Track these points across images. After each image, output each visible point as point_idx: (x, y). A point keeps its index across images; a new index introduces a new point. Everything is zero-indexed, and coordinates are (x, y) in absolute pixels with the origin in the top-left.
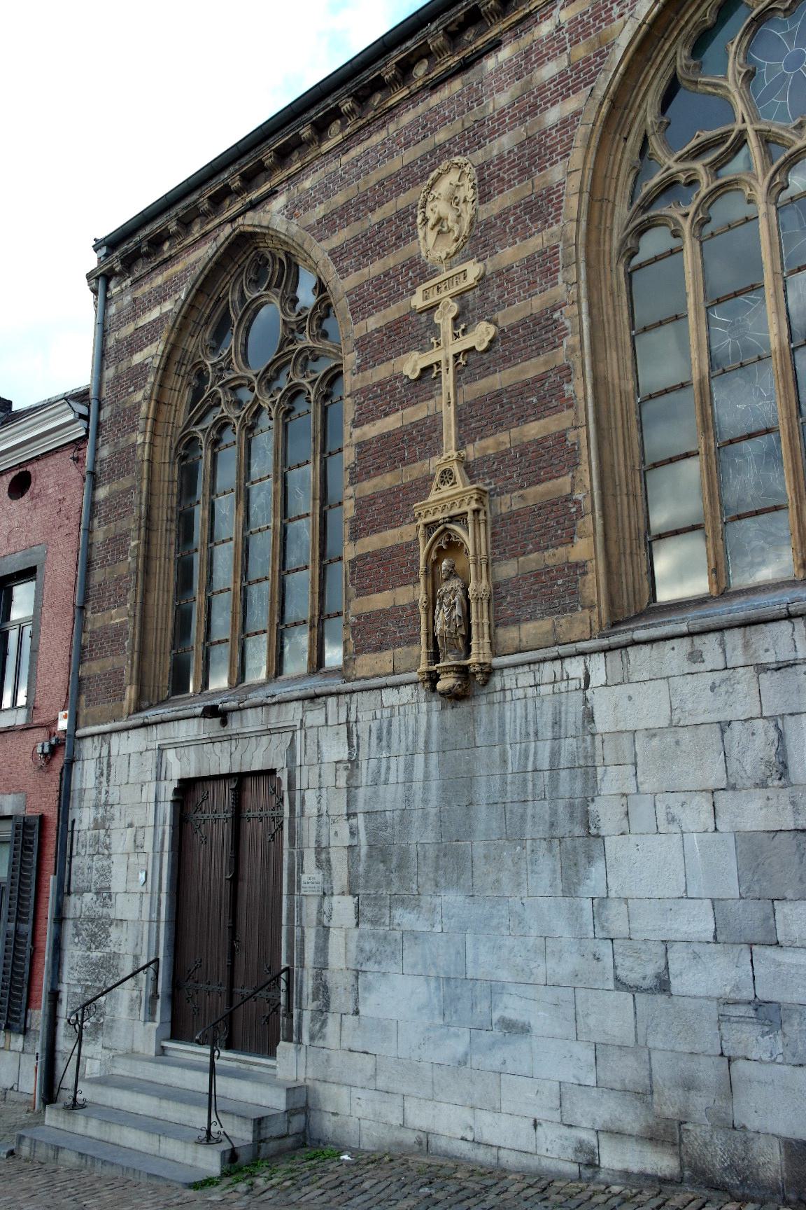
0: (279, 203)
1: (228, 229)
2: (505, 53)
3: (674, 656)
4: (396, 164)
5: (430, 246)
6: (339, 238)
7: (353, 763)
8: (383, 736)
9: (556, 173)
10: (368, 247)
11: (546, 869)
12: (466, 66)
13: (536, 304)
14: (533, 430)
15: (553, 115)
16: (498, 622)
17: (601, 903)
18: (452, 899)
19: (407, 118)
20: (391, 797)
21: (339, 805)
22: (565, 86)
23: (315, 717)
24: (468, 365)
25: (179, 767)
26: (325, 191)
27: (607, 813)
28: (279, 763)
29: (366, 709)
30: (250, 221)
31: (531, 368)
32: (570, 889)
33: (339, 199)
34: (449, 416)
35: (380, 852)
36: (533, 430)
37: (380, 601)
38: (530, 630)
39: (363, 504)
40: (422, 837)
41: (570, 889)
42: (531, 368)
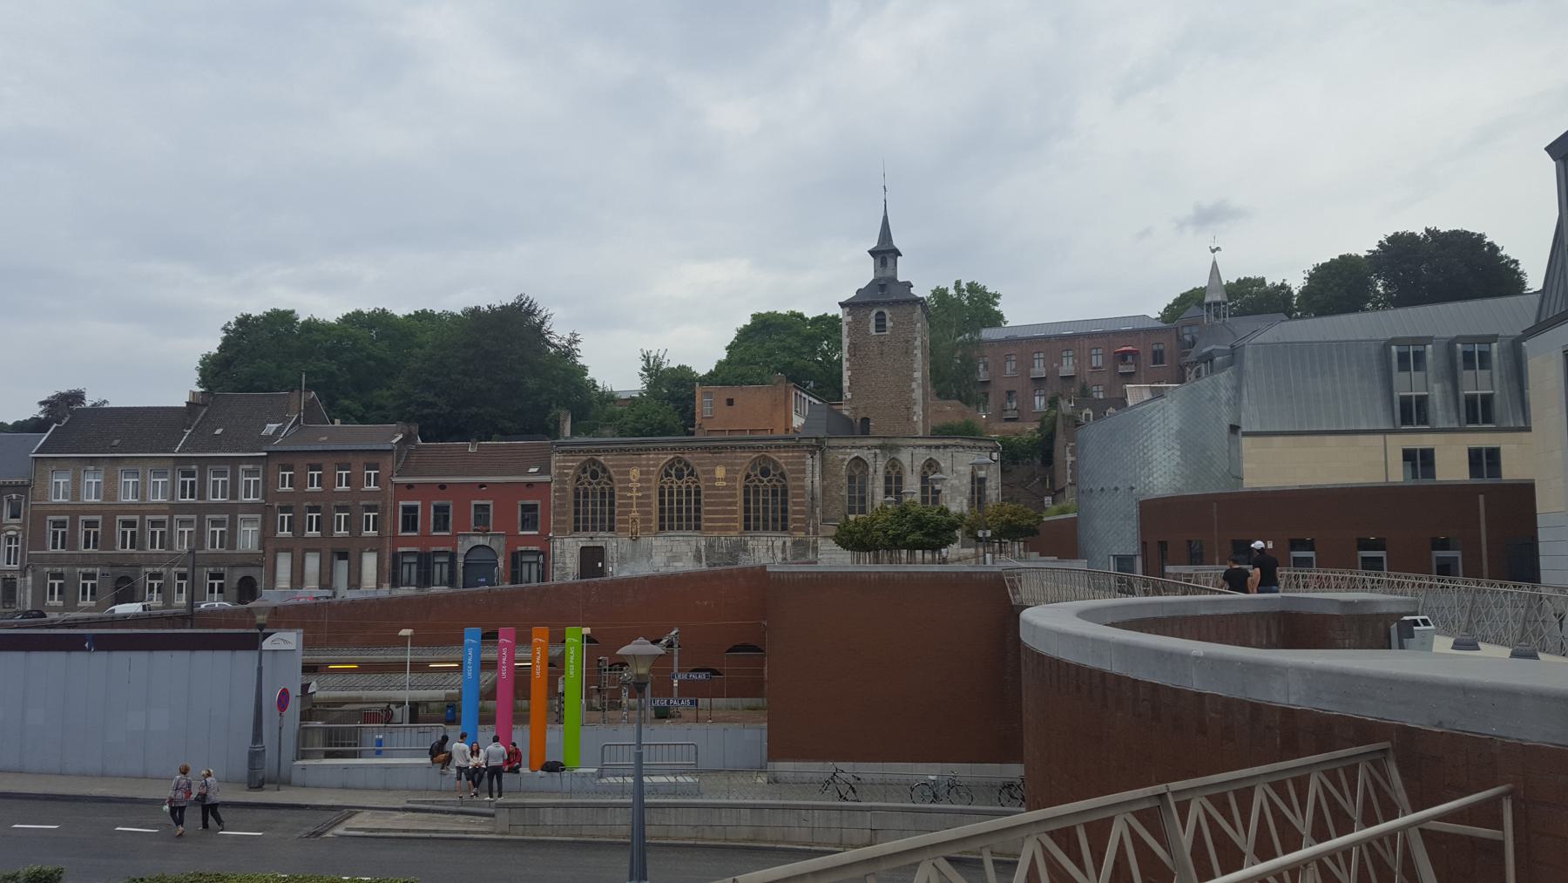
2: (645, 456)
4: (627, 463)
5: (631, 478)
6: (615, 469)
9: (651, 477)
10: (622, 473)
11: (646, 559)
12: (639, 454)
13: (648, 493)
15: (651, 469)
16: (641, 531)
18: (633, 563)
19: (628, 457)
20: (623, 551)
21: (615, 552)
22: (654, 466)
23: (611, 540)
24: (638, 497)
25: (581, 545)
27: (653, 554)
29: (620, 540)
30: (595, 457)
32: (648, 561)
33: (615, 463)
34: (635, 503)
35: (622, 558)
39: (620, 511)
40: (628, 556)
41: (648, 561)
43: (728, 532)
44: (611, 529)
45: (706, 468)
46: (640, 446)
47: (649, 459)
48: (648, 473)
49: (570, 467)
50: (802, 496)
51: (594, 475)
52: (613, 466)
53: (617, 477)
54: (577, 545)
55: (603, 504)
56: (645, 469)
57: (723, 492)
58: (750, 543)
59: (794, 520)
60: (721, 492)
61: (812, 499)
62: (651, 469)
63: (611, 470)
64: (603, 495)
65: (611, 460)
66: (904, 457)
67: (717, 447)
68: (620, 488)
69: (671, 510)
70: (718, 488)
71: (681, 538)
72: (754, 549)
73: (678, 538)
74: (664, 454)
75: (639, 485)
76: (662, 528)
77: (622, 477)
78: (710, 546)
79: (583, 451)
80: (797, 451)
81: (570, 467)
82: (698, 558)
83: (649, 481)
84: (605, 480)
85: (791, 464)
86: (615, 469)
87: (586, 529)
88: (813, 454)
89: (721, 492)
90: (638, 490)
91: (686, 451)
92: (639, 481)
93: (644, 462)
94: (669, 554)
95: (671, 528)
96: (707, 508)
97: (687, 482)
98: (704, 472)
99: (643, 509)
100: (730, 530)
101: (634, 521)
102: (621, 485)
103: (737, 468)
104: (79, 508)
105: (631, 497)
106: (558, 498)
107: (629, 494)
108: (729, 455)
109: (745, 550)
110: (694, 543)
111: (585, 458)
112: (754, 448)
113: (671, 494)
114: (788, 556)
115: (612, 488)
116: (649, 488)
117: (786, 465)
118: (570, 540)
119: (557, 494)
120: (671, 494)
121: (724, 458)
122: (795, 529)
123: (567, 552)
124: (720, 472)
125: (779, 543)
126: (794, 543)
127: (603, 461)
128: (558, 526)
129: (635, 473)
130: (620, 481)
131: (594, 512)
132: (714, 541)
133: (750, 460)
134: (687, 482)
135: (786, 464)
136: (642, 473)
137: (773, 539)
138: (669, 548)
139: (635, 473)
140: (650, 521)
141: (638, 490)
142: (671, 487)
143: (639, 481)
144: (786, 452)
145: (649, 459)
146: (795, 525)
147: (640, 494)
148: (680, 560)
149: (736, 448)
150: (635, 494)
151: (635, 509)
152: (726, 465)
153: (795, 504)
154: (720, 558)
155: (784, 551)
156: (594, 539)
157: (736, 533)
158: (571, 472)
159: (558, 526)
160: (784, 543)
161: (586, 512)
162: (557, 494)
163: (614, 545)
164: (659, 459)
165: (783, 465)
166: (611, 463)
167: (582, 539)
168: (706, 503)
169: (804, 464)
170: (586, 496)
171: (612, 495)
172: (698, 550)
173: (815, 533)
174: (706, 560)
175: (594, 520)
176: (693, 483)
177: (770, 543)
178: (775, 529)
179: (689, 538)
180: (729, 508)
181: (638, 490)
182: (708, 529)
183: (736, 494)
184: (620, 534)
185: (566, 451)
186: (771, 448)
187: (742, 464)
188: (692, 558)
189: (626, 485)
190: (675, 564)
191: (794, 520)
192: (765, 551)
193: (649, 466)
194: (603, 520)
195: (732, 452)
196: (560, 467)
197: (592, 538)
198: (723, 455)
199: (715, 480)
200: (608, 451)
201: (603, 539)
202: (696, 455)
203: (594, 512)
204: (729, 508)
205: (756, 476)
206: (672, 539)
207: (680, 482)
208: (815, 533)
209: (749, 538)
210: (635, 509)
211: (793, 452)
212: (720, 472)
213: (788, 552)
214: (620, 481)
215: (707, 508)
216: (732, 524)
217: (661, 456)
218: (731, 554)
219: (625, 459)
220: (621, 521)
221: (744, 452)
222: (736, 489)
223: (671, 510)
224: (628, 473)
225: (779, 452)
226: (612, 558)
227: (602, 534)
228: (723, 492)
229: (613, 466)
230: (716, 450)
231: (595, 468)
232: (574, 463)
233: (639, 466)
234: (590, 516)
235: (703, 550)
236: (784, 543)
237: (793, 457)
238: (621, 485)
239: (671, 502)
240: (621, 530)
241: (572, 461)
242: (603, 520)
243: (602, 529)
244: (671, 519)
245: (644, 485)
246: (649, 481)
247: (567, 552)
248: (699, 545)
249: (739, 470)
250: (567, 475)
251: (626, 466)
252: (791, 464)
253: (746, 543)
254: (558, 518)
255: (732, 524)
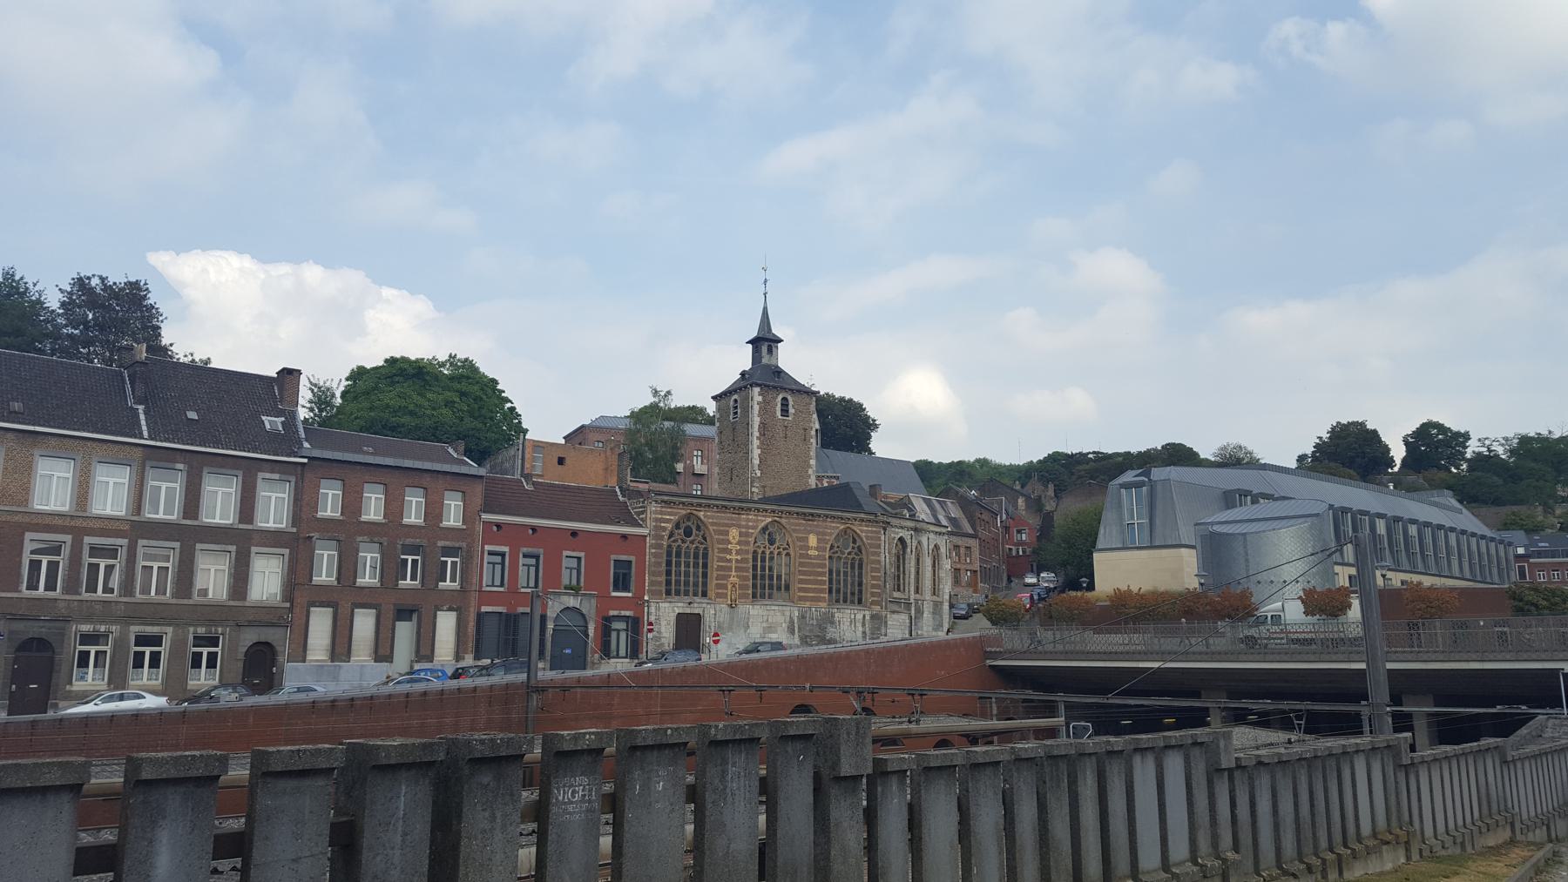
0: (702, 513)
1: (689, 511)
3: (759, 607)
4: (726, 522)
6: (715, 528)
7: (715, 614)
8: (721, 611)
10: (721, 533)
12: (739, 514)
13: (746, 556)
14: (745, 574)
15: (750, 531)
17: (749, 634)
19: (729, 515)
20: (721, 620)
21: (713, 620)
23: (709, 606)
24: (737, 561)
26: (712, 517)
28: (701, 613)
29: (718, 607)
30: (695, 512)
31: (745, 565)
32: (745, 631)
33: (715, 521)
36: (745, 574)
37: (720, 591)
38: (742, 601)
42: (745, 565)
43: (820, 603)
44: (704, 594)
45: (801, 535)
46: (744, 505)
47: (748, 520)
48: (747, 535)
49: (668, 521)
50: (878, 570)
51: (688, 533)
52: (713, 524)
53: (717, 537)
54: (674, 611)
55: (696, 565)
56: (744, 530)
57: (815, 561)
58: (836, 615)
59: (873, 594)
60: (813, 561)
61: (885, 573)
62: (750, 531)
63: (710, 528)
64: (696, 556)
65: (712, 517)
66: (924, 540)
67: (812, 515)
68: (718, 548)
69: (763, 577)
70: (809, 557)
71: (776, 608)
72: (839, 621)
73: (773, 608)
74: (763, 516)
75: (739, 548)
76: (754, 596)
77: (721, 537)
78: (802, 617)
79: (683, 503)
80: (875, 526)
81: (668, 521)
82: (792, 631)
83: (747, 543)
84: (700, 538)
85: (872, 538)
86: (715, 528)
87: (687, 593)
88: (885, 529)
89: (813, 561)
90: (738, 553)
91: (784, 515)
92: (739, 543)
93: (744, 523)
94: (765, 625)
95: (763, 596)
96: (801, 577)
97: (779, 548)
98: (799, 539)
99: (742, 574)
100: (820, 601)
101: (734, 586)
102: (721, 546)
103: (827, 538)
104: (27, 519)
105: (730, 561)
106: (655, 555)
107: (728, 557)
108: (820, 523)
109: (832, 623)
110: (788, 614)
111: (684, 512)
112: (842, 519)
113: (763, 560)
114: (867, 629)
115: (705, 549)
116: (747, 552)
117: (867, 539)
118: (667, 605)
119: (653, 551)
120: (763, 560)
121: (817, 526)
122: (873, 603)
123: (664, 616)
124: (813, 540)
125: (859, 617)
126: (872, 617)
127: (702, 517)
128: (654, 588)
129: (734, 533)
130: (719, 542)
131: (687, 574)
132: (806, 612)
133: (837, 531)
134: (779, 548)
135: (867, 537)
136: (741, 534)
137: (856, 612)
138: (765, 618)
139: (734, 533)
140: (719, 586)
141: (737, 553)
142: (763, 552)
143: (739, 543)
144: (866, 526)
145: (748, 520)
146: (873, 599)
147: (739, 557)
148: (775, 632)
149: (827, 517)
150: (734, 557)
151: (733, 573)
152: (817, 534)
153: (874, 578)
154: (811, 631)
155: (863, 625)
156: (692, 605)
157: (825, 605)
158: (669, 526)
159: (654, 588)
160: (864, 616)
161: (678, 574)
162: (653, 551)
163: (712, 613)
164: (758, 520)
165: (864, 539)
166: (711, 520)
167: (680, 604)
168: (747, 571)
169: (879, 539)
170: (678, 555)
171: (705, 556)
172: (792, 621)
173: (886, 608)
174: (799, 632)
175: (687, 583)
176: (784, 549)
177: (853, 616)
178: (852, 602)
179: (784, 608)
180: (820, 578)
181: (738, 553)
182: (801, 599)
183: (825, 564)
184: (717, 600)
185: (665, 502)
186: (856, 520)
187: (831, 534)
188: (786, 629)
189: (724, 546)
190: (770, 635)
191: (873, 594)
192: (849, 624)
193: (748, 527)
194: (696, 584)
195: (823, 521)
196: (657, 520)
197: (690, 603)
198: (815, 523)
199: (808, 548)
200: (709, 506)
201: (700, 605)
202: (792, 521)
203: (687, 574)
204: (820, 578)
205: (838, 547)
206: (768, 608)
207: (772, 547)
208: (886, 608)
209: (836, 610)
210: (733, 573)
211: (872, 526)
212: (813, 540)
213: (867, 626)
214: (719, 542)
215: (801, 577)
216: (822, 595)
217: (759, 518)
218: (820, 626)
219: (725, 517)
220: (719, 586)
221: (833, 522)
222: (825, 559)
223: (763, 577)
224: (727, 533)
225: (861, 525)
226: (710, 627)
227: (697, 599)
228: (815, 561)
229: (713, 524)
230: (810, 518)
231: (690, 524)
232: (672, 516)
233: (739, 526)
234: (682, 578)
235: (796, 621)
236: (864, 616)
237: (872, 532)
238: (721, 546)
239: (763, 568)
240: (718, 595)
241: (670, 514)
242: (696, 584)
243: (695, 594)
244: (763, 587)
245: (743, 547)
246: (747, 543)
247: (664, 616)
248: (792, 615)
249: (829, 540)
250: (664, 529)
251: (727, 525)
252: (872, 538)
253: (833, 616)
254: (654, 579)
255: (822, 595)
